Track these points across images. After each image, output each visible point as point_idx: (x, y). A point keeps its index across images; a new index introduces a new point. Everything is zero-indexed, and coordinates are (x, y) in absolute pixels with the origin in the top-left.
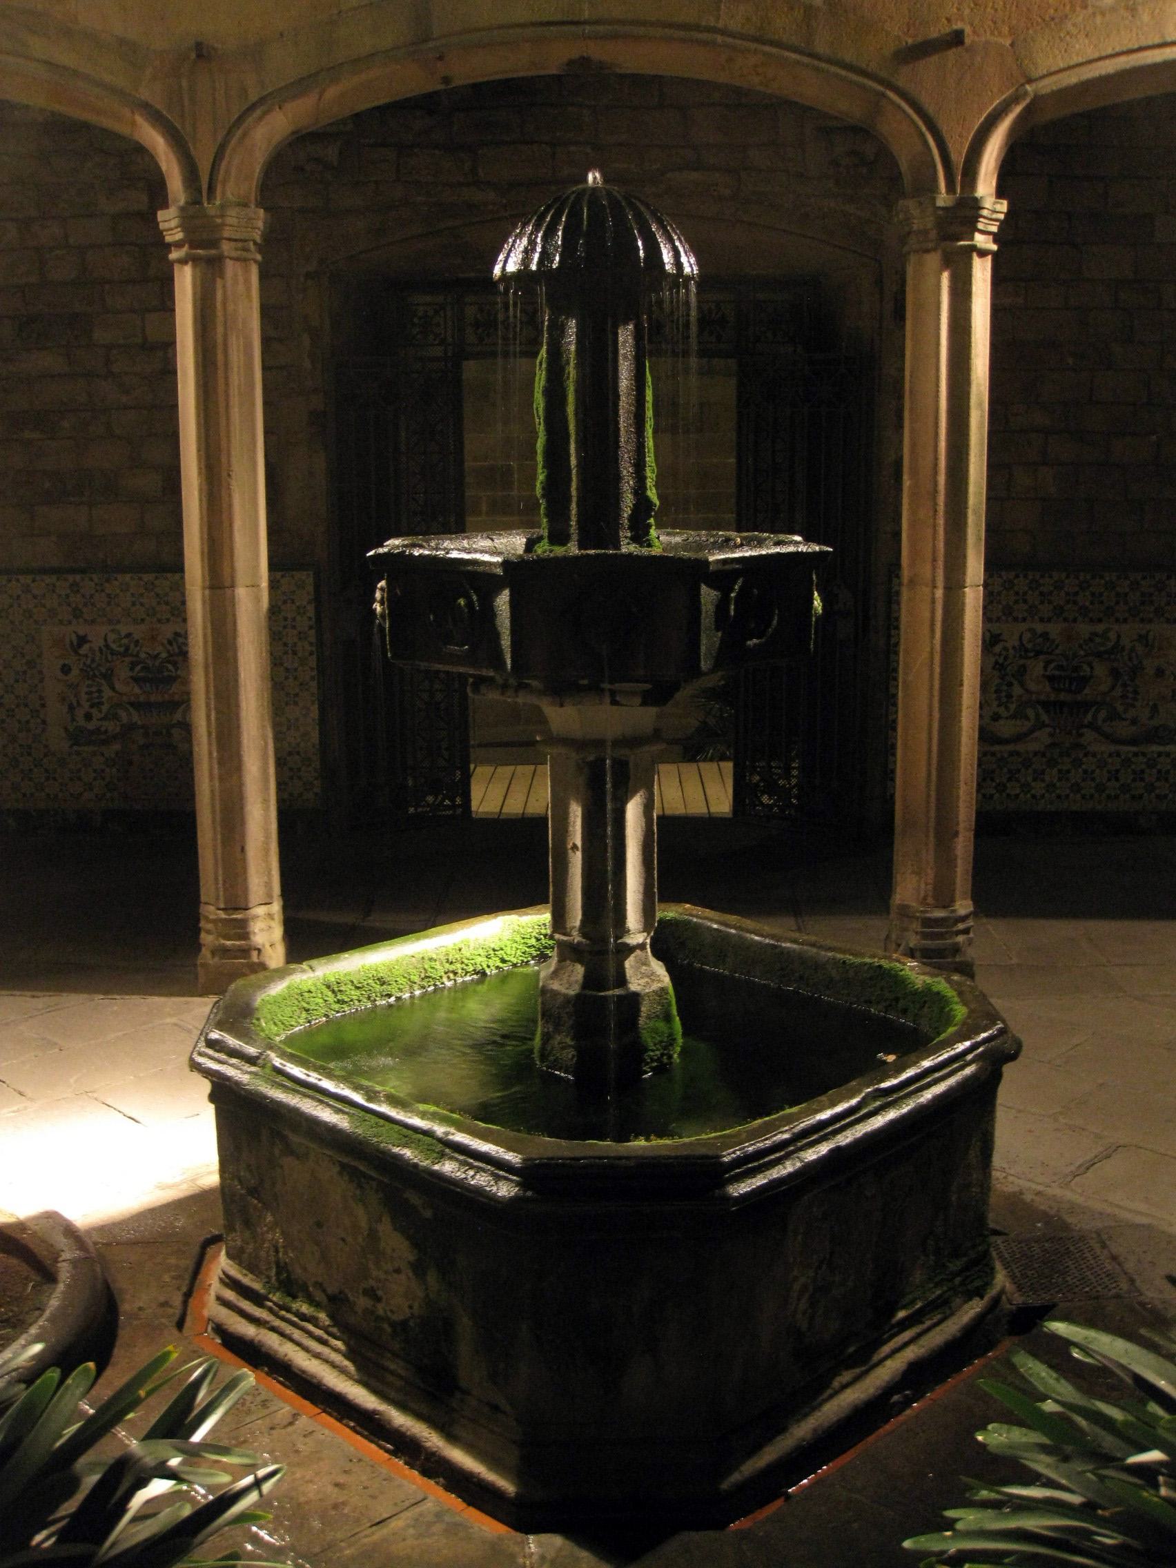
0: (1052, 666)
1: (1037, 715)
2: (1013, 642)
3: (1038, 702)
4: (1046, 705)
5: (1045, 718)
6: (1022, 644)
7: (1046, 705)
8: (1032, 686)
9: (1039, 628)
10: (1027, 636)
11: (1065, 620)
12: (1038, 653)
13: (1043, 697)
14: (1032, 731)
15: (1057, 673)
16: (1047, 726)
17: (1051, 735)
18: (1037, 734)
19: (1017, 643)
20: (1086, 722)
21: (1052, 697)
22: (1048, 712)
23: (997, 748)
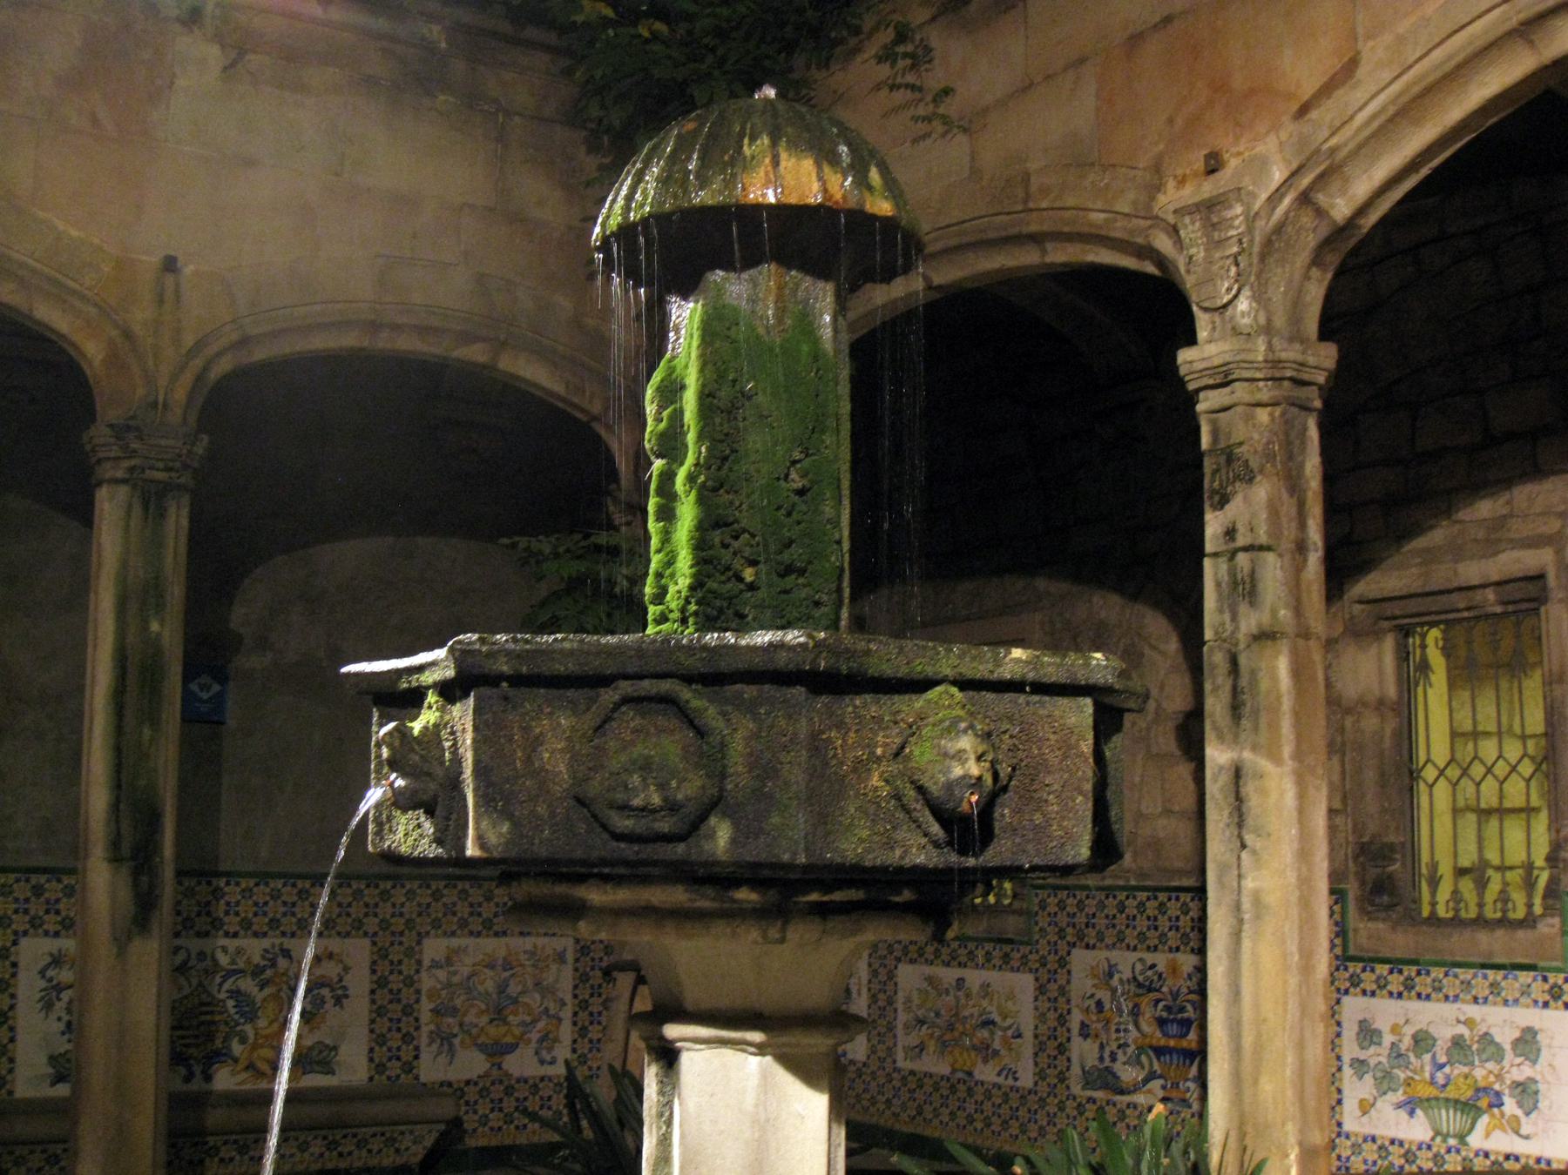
0: (1161, 1005)
1: (1151, 1064)
2: (1127, 974)
3: (1151, 1047)
4: (1159, 1051)
5: (1156, 1066)
6: (1135, 978)
7: (1159, 1051)
8: (1145, 1028)
9: (1150, 958)
10: (1139, 967)
11: (1170, 950)
12: (1150, 990)
13: (1154, 1042)
14: (1146, 1081)
15: (1165, 1014)
16: (1160, 1077)
17: (1164, 1087)
18: (1150, 1085)
19: (1130, 976)
20: (1191, 1076)
21: (1163, 1042)
22: (1159, 1059)
23: (1118, 1098)
